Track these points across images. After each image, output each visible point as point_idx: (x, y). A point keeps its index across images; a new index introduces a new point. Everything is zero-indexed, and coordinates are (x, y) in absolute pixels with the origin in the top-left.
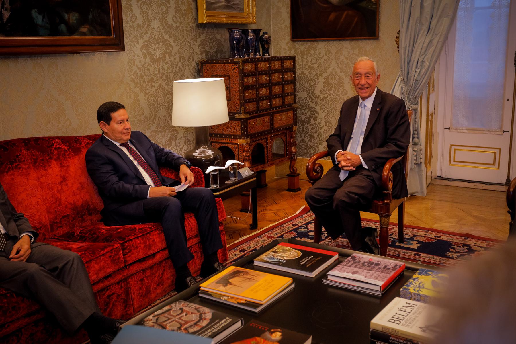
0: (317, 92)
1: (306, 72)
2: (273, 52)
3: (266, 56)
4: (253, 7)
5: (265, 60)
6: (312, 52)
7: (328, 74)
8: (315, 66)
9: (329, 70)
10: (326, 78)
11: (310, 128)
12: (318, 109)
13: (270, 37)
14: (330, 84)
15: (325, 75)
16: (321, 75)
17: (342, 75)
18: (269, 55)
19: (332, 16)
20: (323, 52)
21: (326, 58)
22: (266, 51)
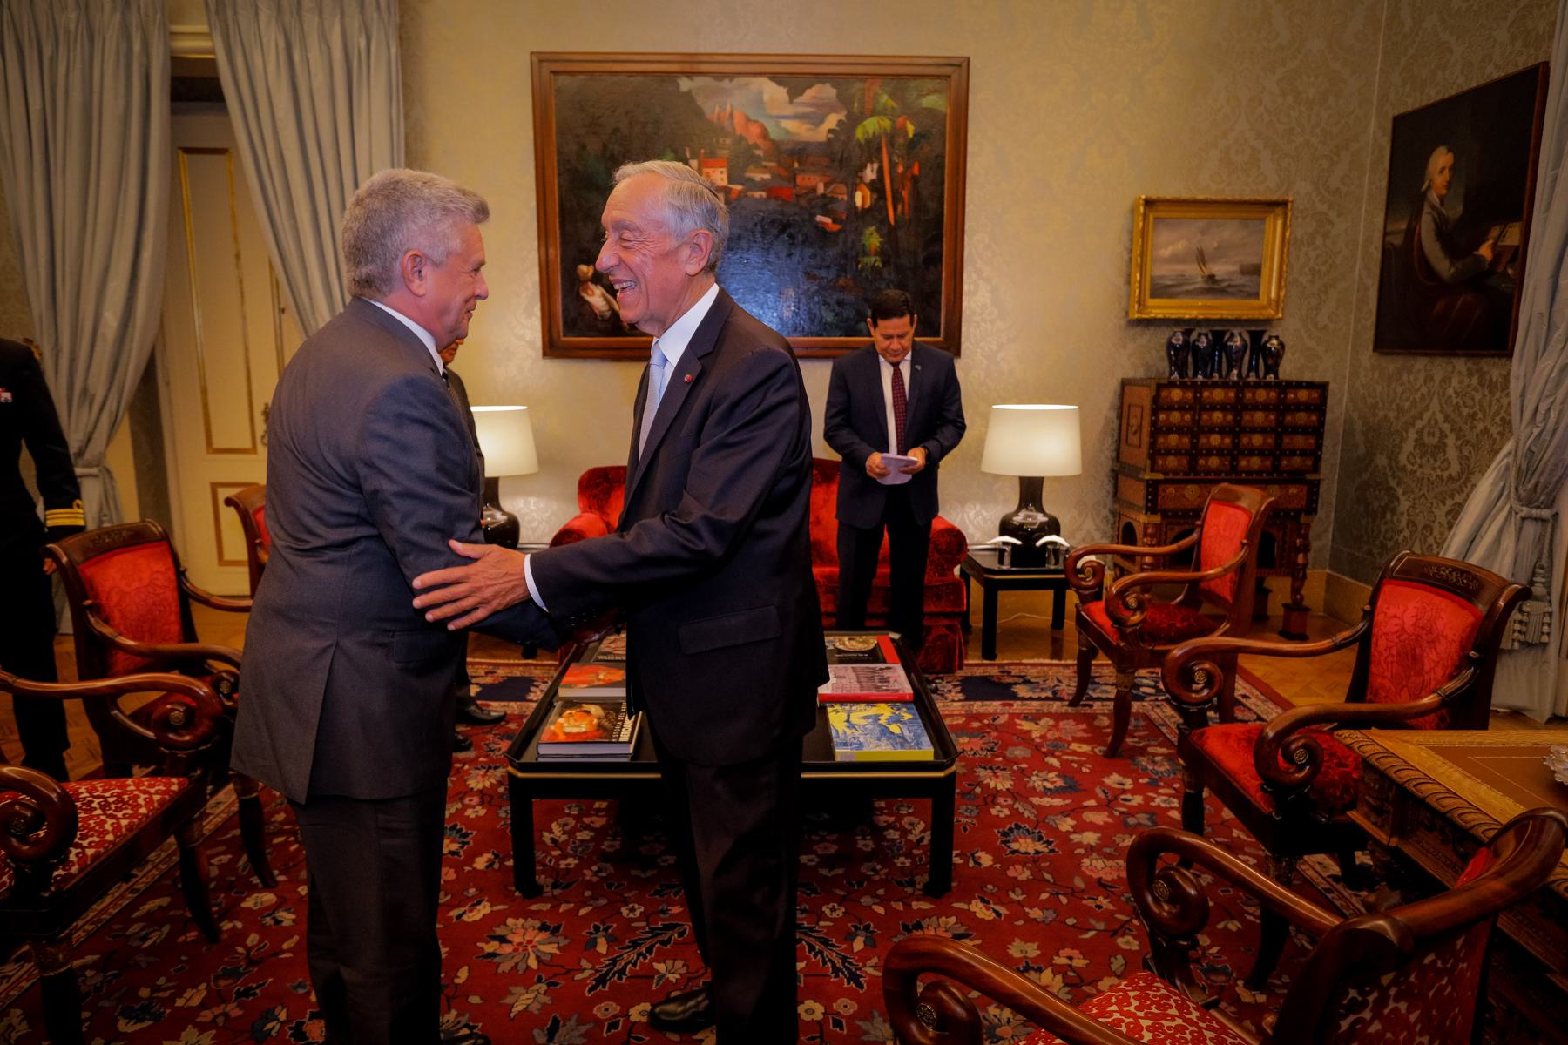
0: (1403, 458)
1: (1392, 415)
2: (1289, 369)
3: (1271, 377)
4: (1279, 288)
5: (1268, 386)
6: (1405, 378)
7: (1425, 422)
8: (1407, 404)
9: (1427, 416)
10: (1422, 429)
11: (1383, 528)
12: (1400, 491)
13: (1282, 345)
14: (1424, 445)
15: (1419, 424)
16: (1413, 425)
17: (1446, 427)
18: (1276, 376)
19: (1439, 306)
20: (1421, 381)
21: (1424, 390)
22: (1273, 368)
